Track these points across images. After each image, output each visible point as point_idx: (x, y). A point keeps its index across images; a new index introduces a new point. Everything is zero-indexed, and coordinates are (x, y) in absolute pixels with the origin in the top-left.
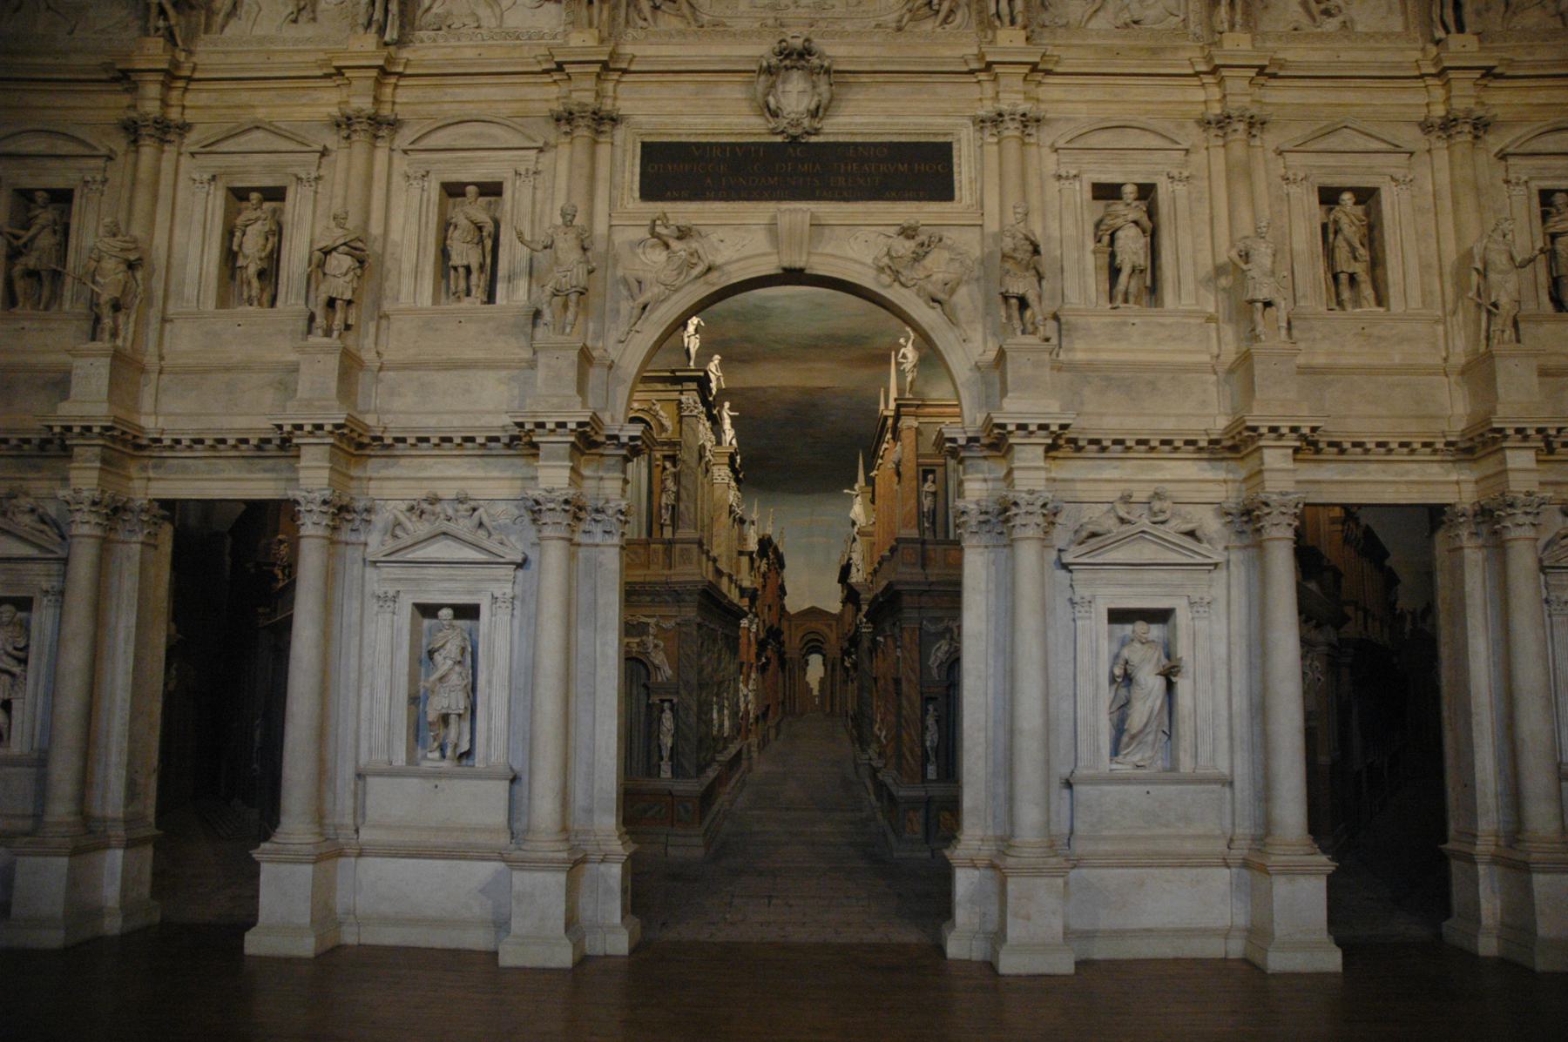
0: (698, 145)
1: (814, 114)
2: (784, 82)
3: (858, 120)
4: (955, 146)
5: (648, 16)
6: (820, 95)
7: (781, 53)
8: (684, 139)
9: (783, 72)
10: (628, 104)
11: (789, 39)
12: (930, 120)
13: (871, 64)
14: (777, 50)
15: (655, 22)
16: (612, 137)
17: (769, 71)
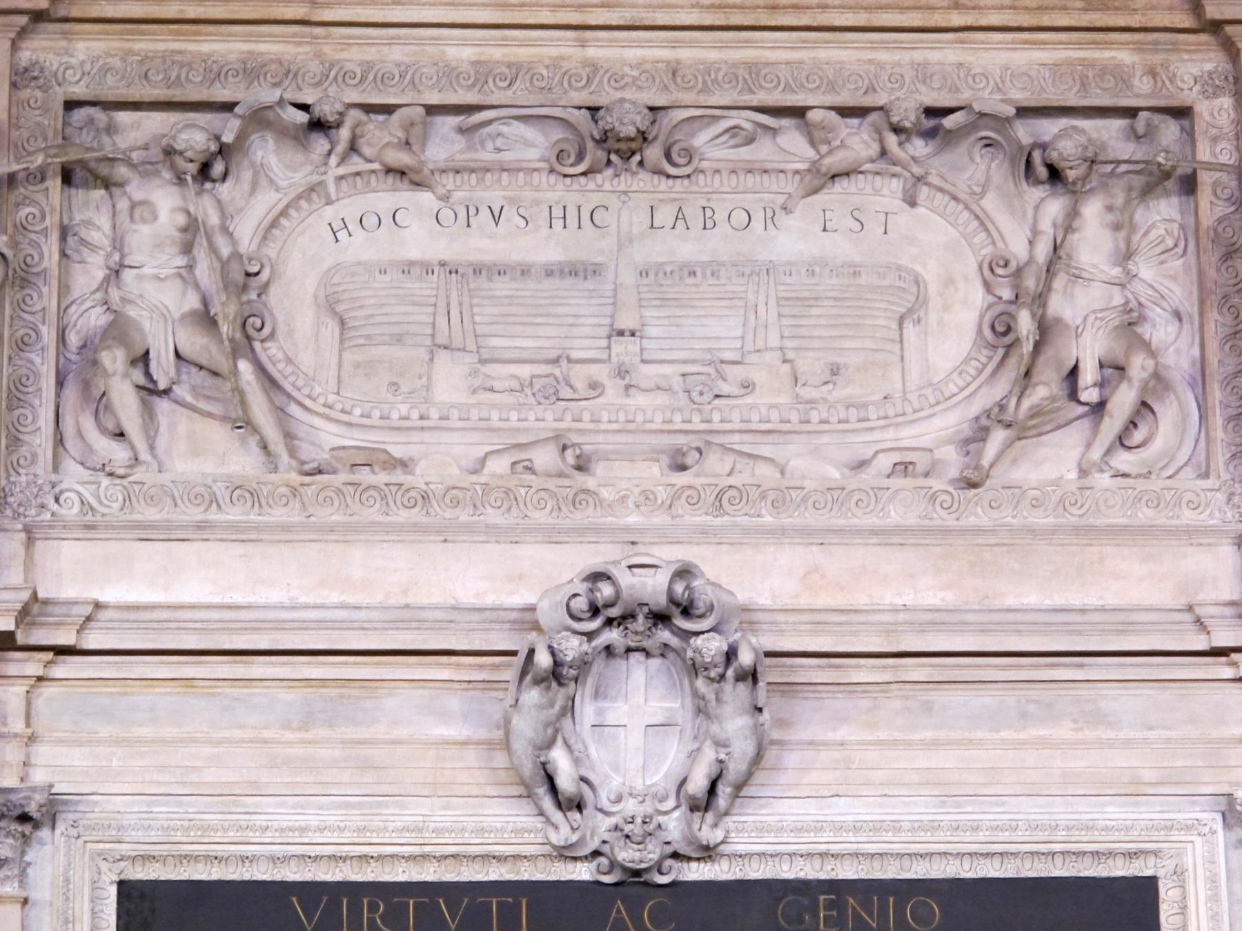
0: (310, 891)
1: (704, 803)
2: (597, 695)
3: (846, 810)
4: (1168, 895)
5: (133, 427)
6: (720, 744)
7: (595, 611)
8: (262, 873)
9: (599, 665)
10: (77, 757)
11: (626, 580)
12: (1085, 810)
13: (890, 630)
14: (581, 604)
15: (152, 448)
16: (23, 873)
17: (556, 674)
